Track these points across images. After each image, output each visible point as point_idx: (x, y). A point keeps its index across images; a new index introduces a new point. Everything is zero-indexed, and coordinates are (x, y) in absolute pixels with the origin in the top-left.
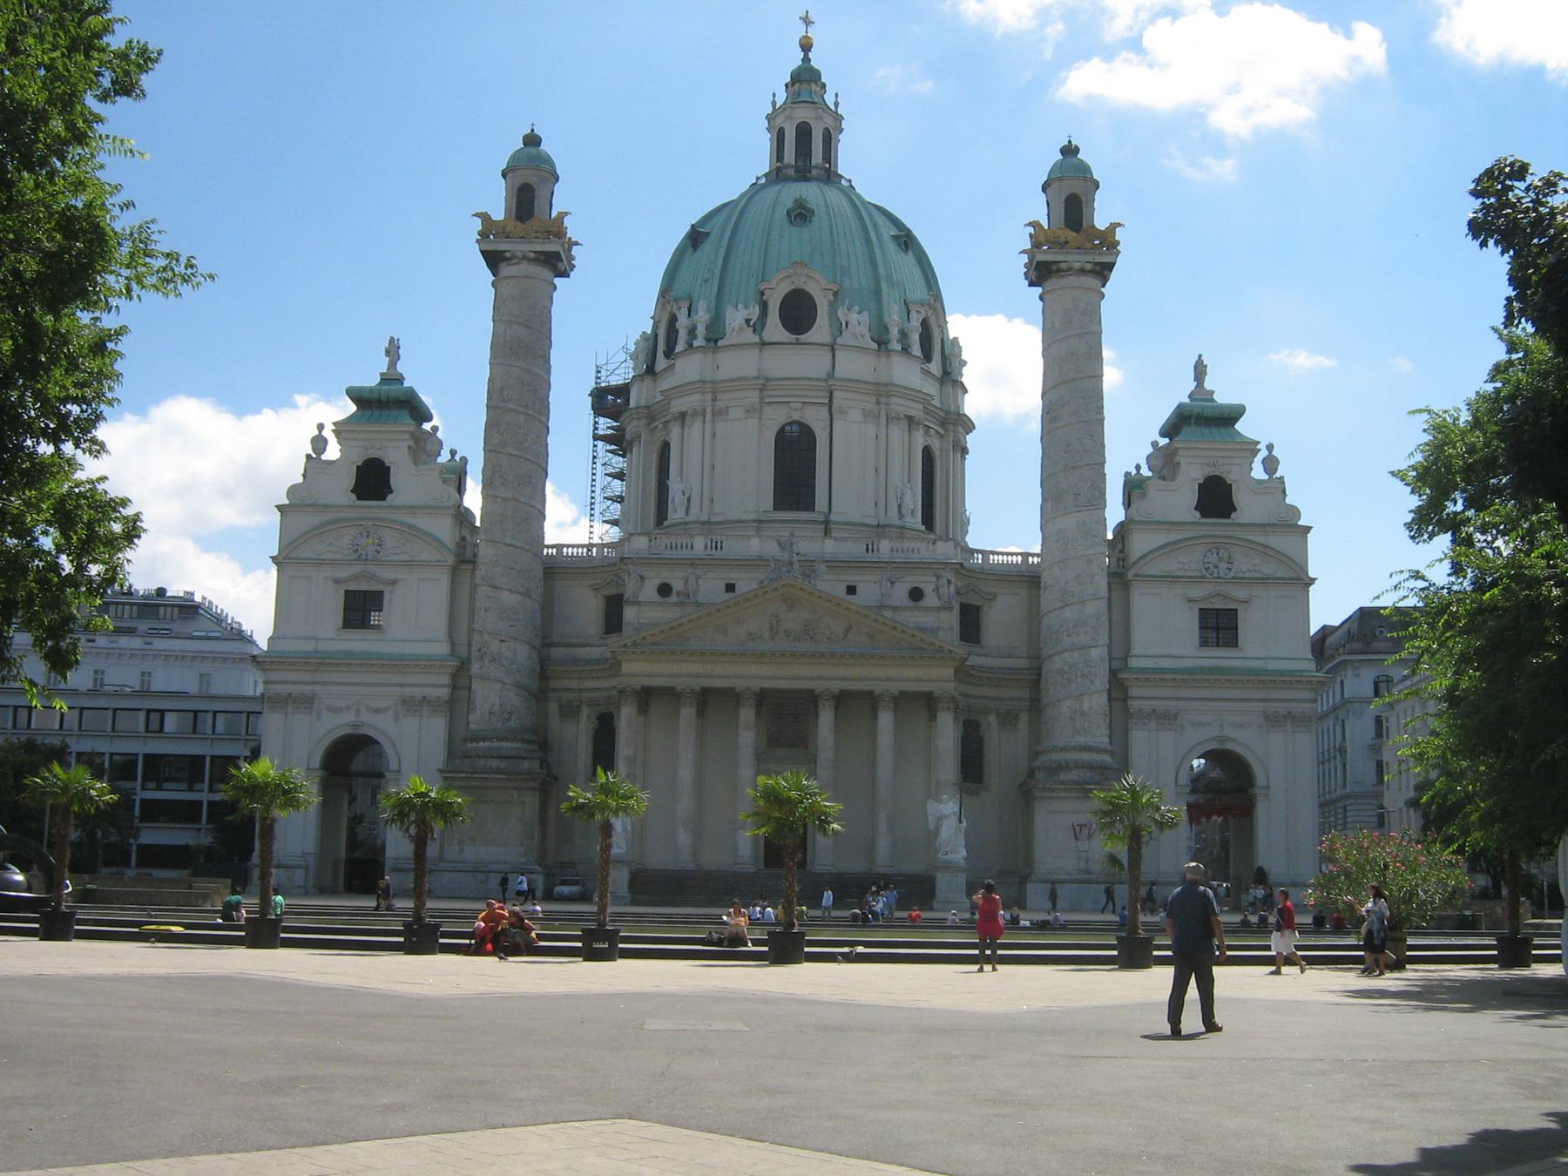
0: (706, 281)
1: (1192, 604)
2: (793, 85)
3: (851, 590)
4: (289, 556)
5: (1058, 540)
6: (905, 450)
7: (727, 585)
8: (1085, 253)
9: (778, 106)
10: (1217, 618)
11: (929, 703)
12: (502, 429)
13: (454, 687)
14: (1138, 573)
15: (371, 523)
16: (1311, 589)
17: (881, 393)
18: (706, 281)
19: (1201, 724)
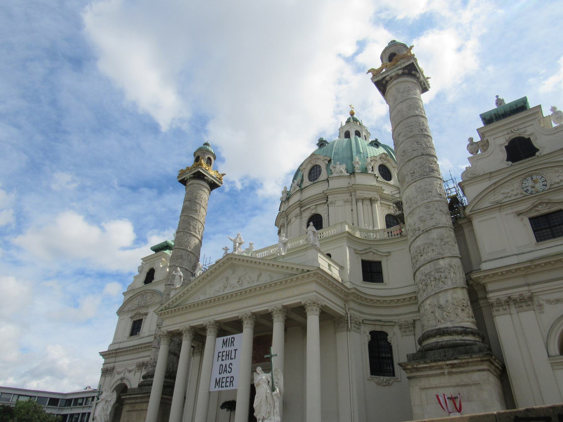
1: (521, 216)
8: (396, 67)
15: (143, 293)
17: (351, 191)
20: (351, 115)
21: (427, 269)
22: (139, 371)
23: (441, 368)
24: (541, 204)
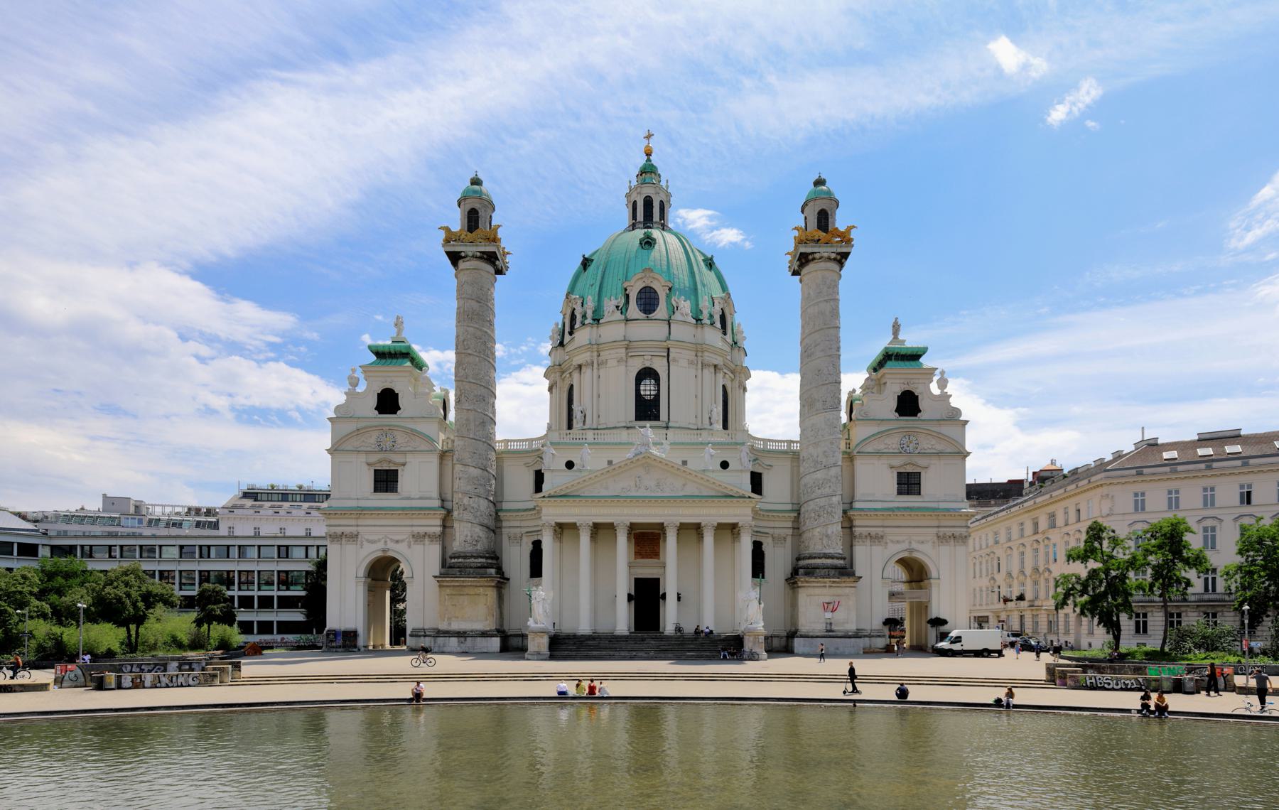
0: (592, 285)
1: (893, 469)
2: (641, 175)
3: (685, 463)
4: (341, 448)
5: (812, 430)
6: (711, 385)
7: (608, 461)
9: (633, 187)
10: (908, 478)
11: (732, 529)
13: (444, 527)
14: (861, 451)
18: (592, 285)
19: (898, 542)
20: (647, 155)
21: (822, 502)
23: (825, 583)
24: (909, 464)
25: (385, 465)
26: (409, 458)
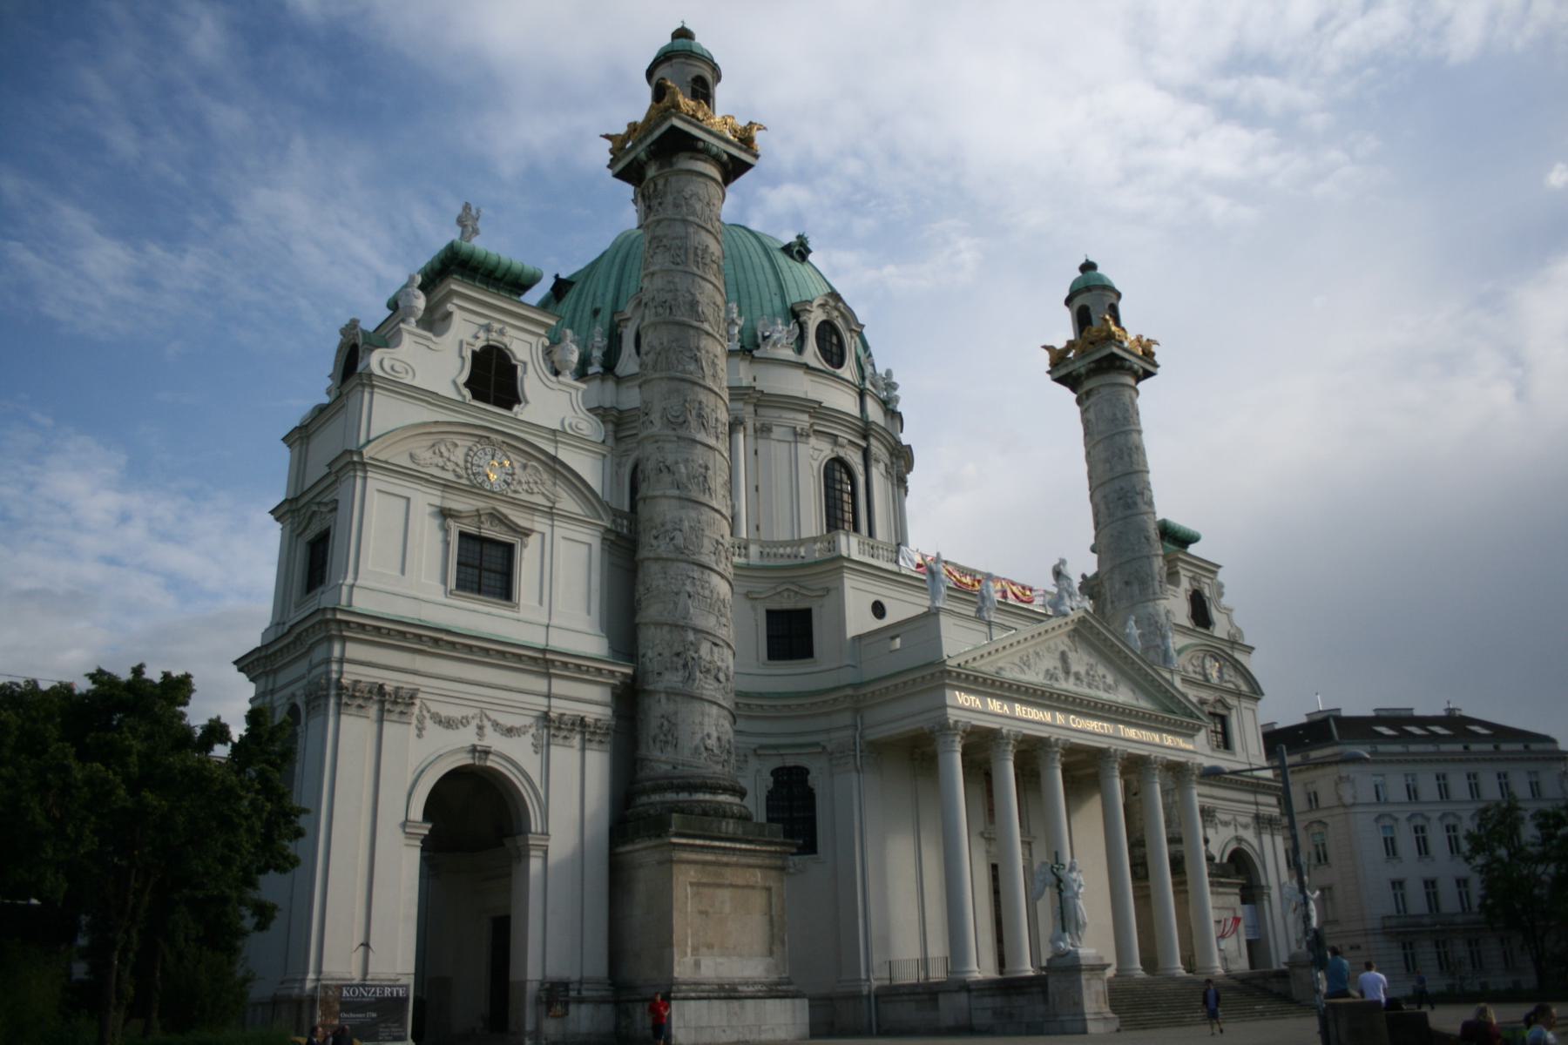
12: (698, 354)
15: (500, 438)
16: (1260, 703)
22: (561, 741)
25: (487, 525)
26: (540, 524)
